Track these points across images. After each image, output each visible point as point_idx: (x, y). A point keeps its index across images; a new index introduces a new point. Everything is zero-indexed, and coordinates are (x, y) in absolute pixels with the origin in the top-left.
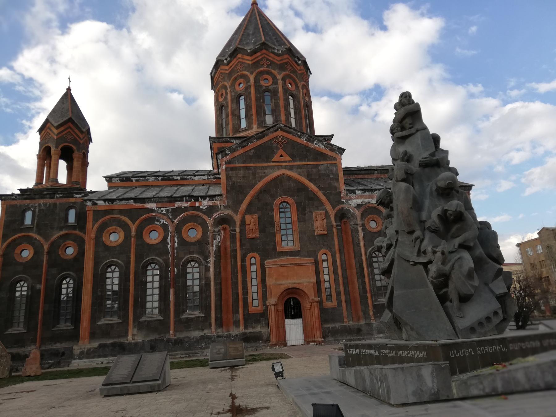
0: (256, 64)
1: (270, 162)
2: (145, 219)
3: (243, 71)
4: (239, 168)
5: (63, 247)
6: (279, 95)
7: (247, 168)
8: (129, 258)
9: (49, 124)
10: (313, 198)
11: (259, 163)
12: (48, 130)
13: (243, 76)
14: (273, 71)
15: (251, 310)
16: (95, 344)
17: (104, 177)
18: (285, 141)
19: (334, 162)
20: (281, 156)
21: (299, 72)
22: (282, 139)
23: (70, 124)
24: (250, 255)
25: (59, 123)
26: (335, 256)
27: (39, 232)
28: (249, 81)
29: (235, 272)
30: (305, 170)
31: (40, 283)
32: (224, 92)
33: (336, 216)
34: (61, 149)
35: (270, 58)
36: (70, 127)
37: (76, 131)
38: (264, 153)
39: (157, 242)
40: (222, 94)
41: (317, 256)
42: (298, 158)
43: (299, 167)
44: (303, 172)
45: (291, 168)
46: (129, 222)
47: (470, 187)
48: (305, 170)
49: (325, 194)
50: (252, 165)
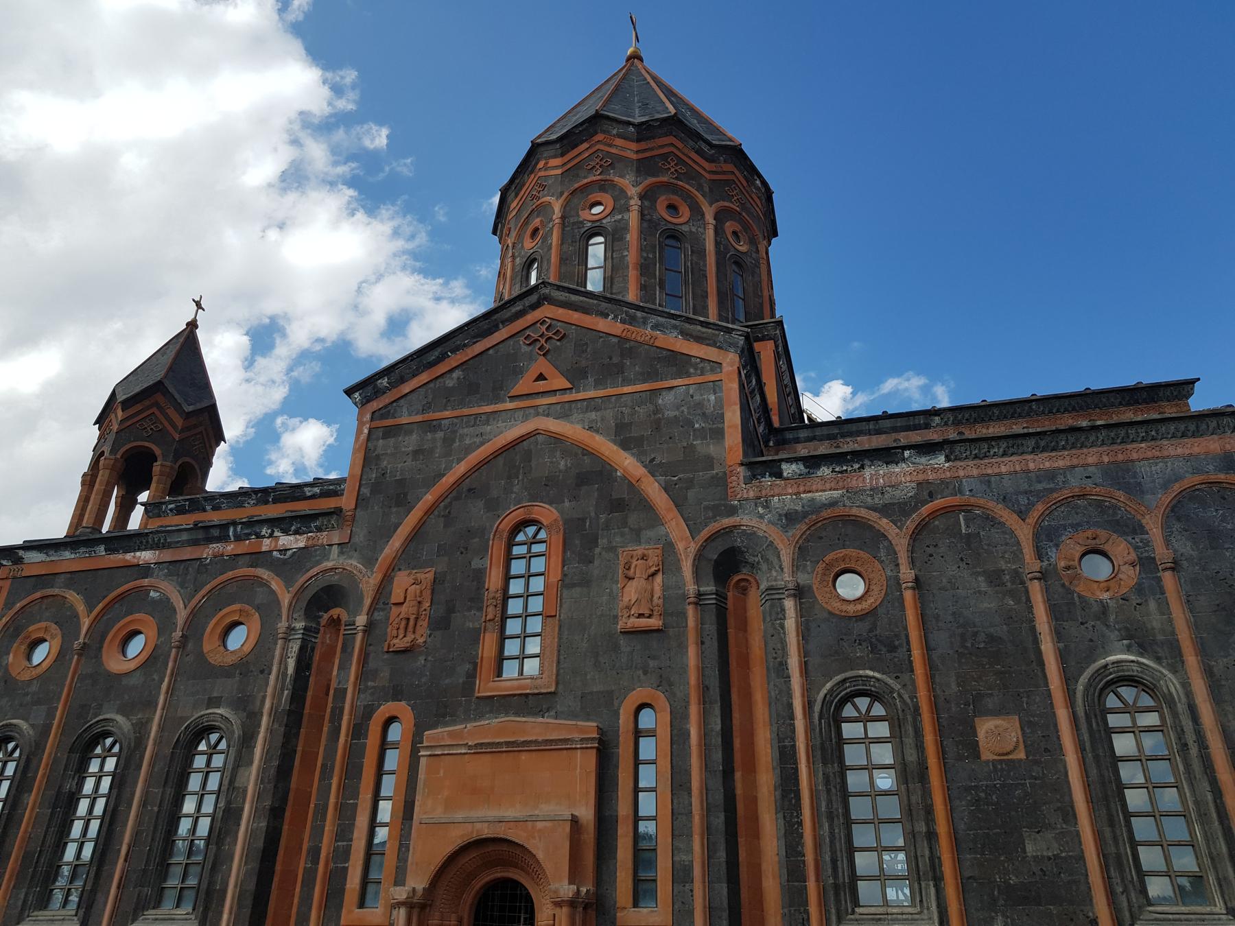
2: (121, 598)
6: (628, 237)
7: (430, 426)
8: (51, 714)
10: (623, 503)
20: (541, 377)
26: (685, 717)
30: (609, 414)
33: (699, 557)
35: (613, 150)
36: (157, 404)
41: (616, 714)
45: (565, 412)
46: (81, 608)
48: (609, 414)
50: (447, 414)
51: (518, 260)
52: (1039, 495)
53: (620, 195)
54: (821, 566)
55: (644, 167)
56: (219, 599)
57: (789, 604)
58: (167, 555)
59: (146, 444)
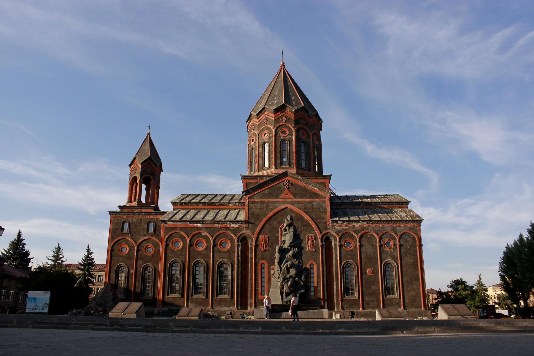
0: (277, 120)
4: (257, 202)
7: (262, 202)
9: (136, 161)
10: (306, 225)
13: (268, 129)
14: (290, 126)
20: (287, 194)
22: (288, 182)
23: (149, 161)
24: (262, 261)
28: (272, 133)
31: (133, 269)
32: (254, 138)
36: (149, 163)
37: (153, 165)
39: (202, 249)
40: (253, 140)
43: (299, 202)
45: (293, 203)
47: (421, 221)
48: (303, 205)
51: (260, 140)
52: (381, 231)
53: (290, 130)
55: (297, 122)
57: (338, 248)
58: (205, 226)
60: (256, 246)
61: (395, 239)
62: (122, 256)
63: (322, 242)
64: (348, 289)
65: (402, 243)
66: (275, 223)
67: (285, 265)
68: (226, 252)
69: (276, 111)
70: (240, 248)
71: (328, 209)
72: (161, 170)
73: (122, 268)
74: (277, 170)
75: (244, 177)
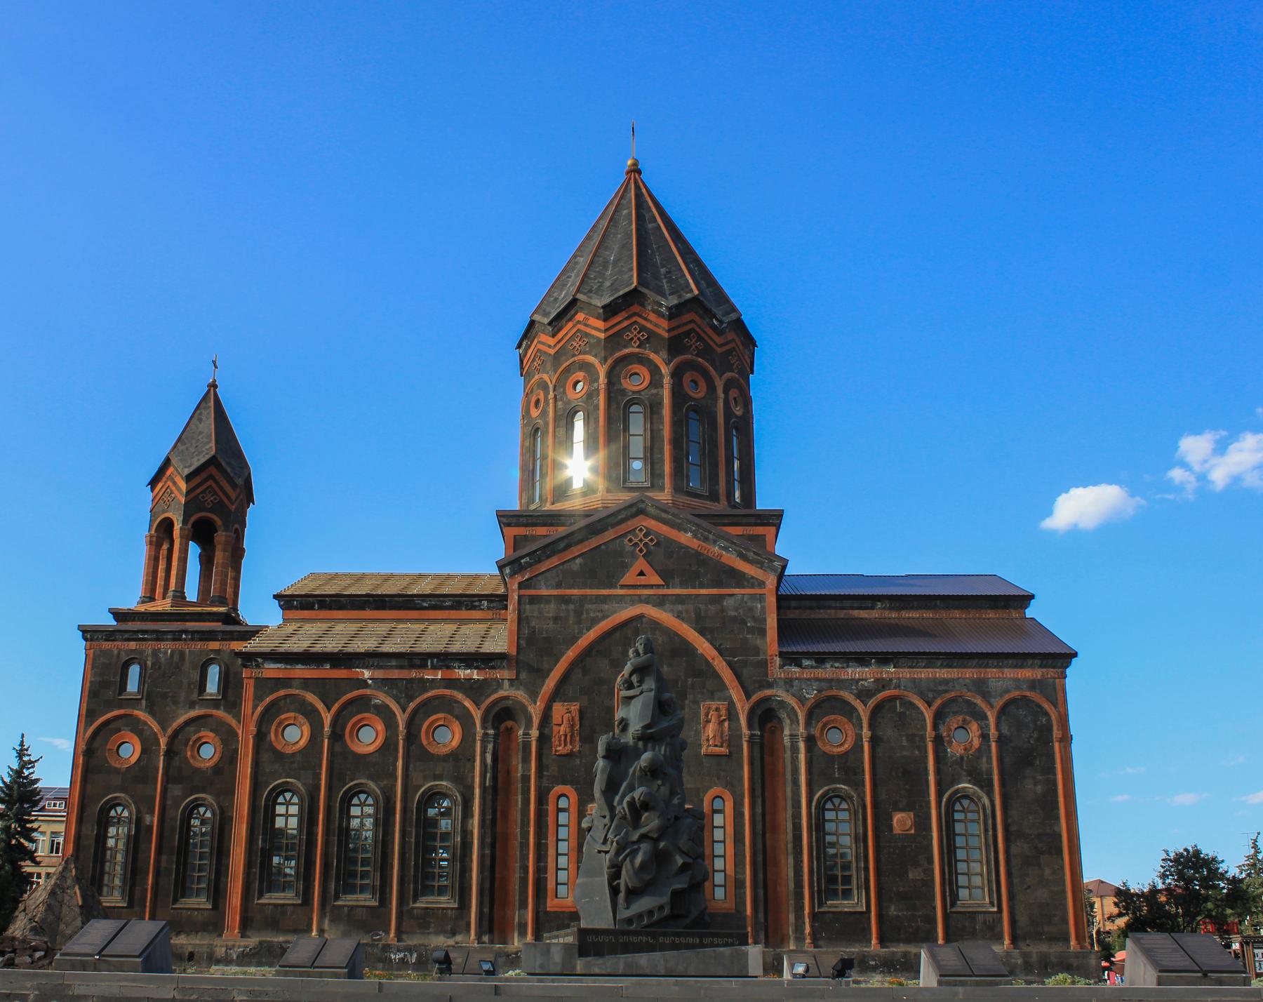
0: (614, 341)
1: (615, 587)
2: (351, 702)
3: (586, 353)
5: (195, 742)
8: (317, 777)
9: (170, 470)
10: (703, 671)
11: (591, 588)
12: (169, 483)
13: (585, 366)
14: (652, 356)
15: (551, 904)
16: (253, 941)
17: (275, 597)
18: (651, 540)
19: (758, 591)
20: (641, 574)
21: (719, 350)
22: (646, 535)
23: (212, 470)
24: (558, 789)
25: (192, 469)
26: (742, 805)
27: (151, 710)
28: (597, 380)
29: (525, 823)
32: (542, 397)
33: (751, 713)
34: (193, 526)
35: (648, 325)
36: (211, 477)
38: (604, 568)
39: (372, 749)
40: (538, 402)
41: (702, 801)
42: (677, 580)
43: (679, 599)
44: (687, 611)
45: (660, 602)
47: (1064, 658)
48: (691, 607)
49: (730, 664)
51: (560, 404)
53: (655, 371)
54: (820, 725)
55: (675, 346)
56: (427, 708)
57: (802, 745)
58: (380, 674)
59: (209, 515)
60: (544, 739)
61: (985, 718)
62: (117, 771)
63: (750, 726)
64: (832, 879)
65: (1005, 730)
66: (604, 664)
67: (627, 799)
68: (445, 758)
69: (610, 311)
70: (490, 746)
71: (772, 622)
72: (250, 498)
73: (119, 809)
74: (610, 496)
75: (506, 519)
